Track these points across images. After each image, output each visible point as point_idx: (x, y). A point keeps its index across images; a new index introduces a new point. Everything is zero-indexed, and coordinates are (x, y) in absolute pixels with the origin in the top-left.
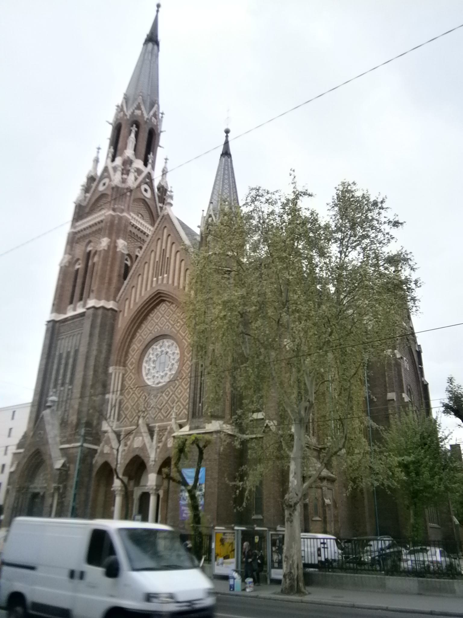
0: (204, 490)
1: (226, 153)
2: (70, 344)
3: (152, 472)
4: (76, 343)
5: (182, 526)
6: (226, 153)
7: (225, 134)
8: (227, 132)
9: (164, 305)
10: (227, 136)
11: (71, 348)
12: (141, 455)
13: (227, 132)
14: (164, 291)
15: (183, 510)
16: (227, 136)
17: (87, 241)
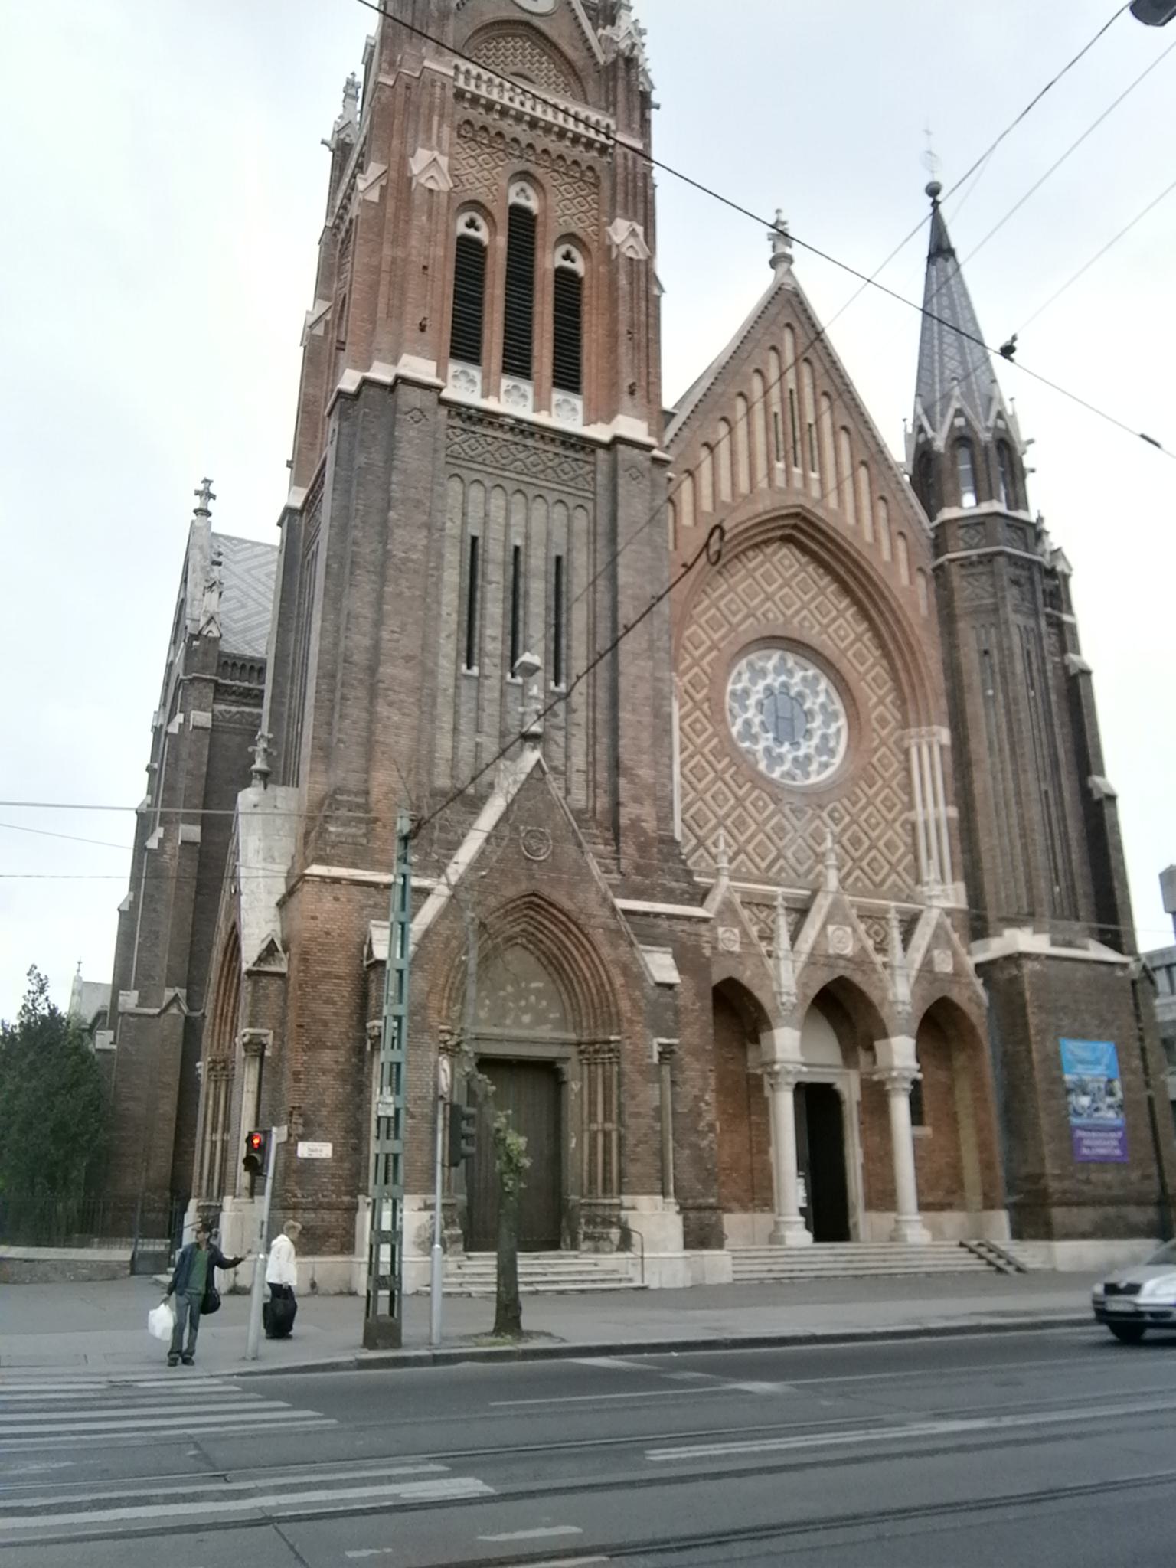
0: (1120, 1095)
1: (941, 250)
2: (517, 518)
3: (902, 1032)
4: (549, 534)
5: (1082, 1176)
6: (941, 250)
7: (931, 200)
8: (933, 191)
9: (784, 551)
10: (935, 204)
11: (527, 537)
12: (857, 978)
13: (933, 191)
14: (820, 519)
15: (1081, 1139)
16: (935, 204)
17: (520, 165)
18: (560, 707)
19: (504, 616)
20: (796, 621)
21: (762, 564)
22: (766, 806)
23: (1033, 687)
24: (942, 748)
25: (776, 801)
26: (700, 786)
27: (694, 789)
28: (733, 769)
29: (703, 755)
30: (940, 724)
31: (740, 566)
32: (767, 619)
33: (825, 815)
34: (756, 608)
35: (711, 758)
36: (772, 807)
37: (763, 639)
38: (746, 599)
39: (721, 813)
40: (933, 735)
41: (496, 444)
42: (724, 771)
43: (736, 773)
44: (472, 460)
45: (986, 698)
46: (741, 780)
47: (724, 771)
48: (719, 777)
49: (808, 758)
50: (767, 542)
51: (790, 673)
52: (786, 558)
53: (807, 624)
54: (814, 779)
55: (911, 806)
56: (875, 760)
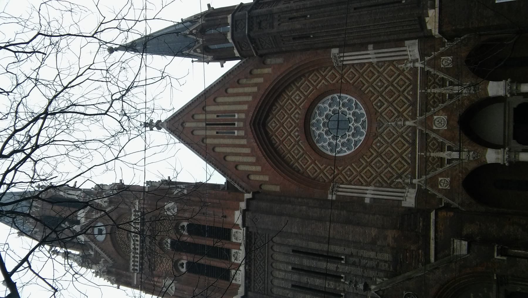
18: (352, 260)
19: (319, 278)
20: (297, 122)
21: (276, 136)
22: (379, 141)
23: (305, 16)
24: (340, 52)
25: (376, 136)
26: (375, 174)
27: (376, 177)
28: (364, 156)
29: (361, 171)
30: (330, 52)
31: (279, 147)
32: (298, 136)
33: (380, 111)
34: (295, 141)
35: (361, 168)
36: (379, 138)
37: (307, 139)
38: (292, 145)
39: (385, 165)
40: (335, 56)
41: (256, 272)
42: (366, 162)
43: (366, 156)
44: (264, 283)
45: (314, 37)
46: (370, 154)
47: (366, 162)
48: (369, 164)
49: (354, 114)
50: (267, 133)
51: (320, 135)
52: (272, 125)
53: (297, 116)
54: (363, 111)
55: (371, 64)
56: (351, 82)
